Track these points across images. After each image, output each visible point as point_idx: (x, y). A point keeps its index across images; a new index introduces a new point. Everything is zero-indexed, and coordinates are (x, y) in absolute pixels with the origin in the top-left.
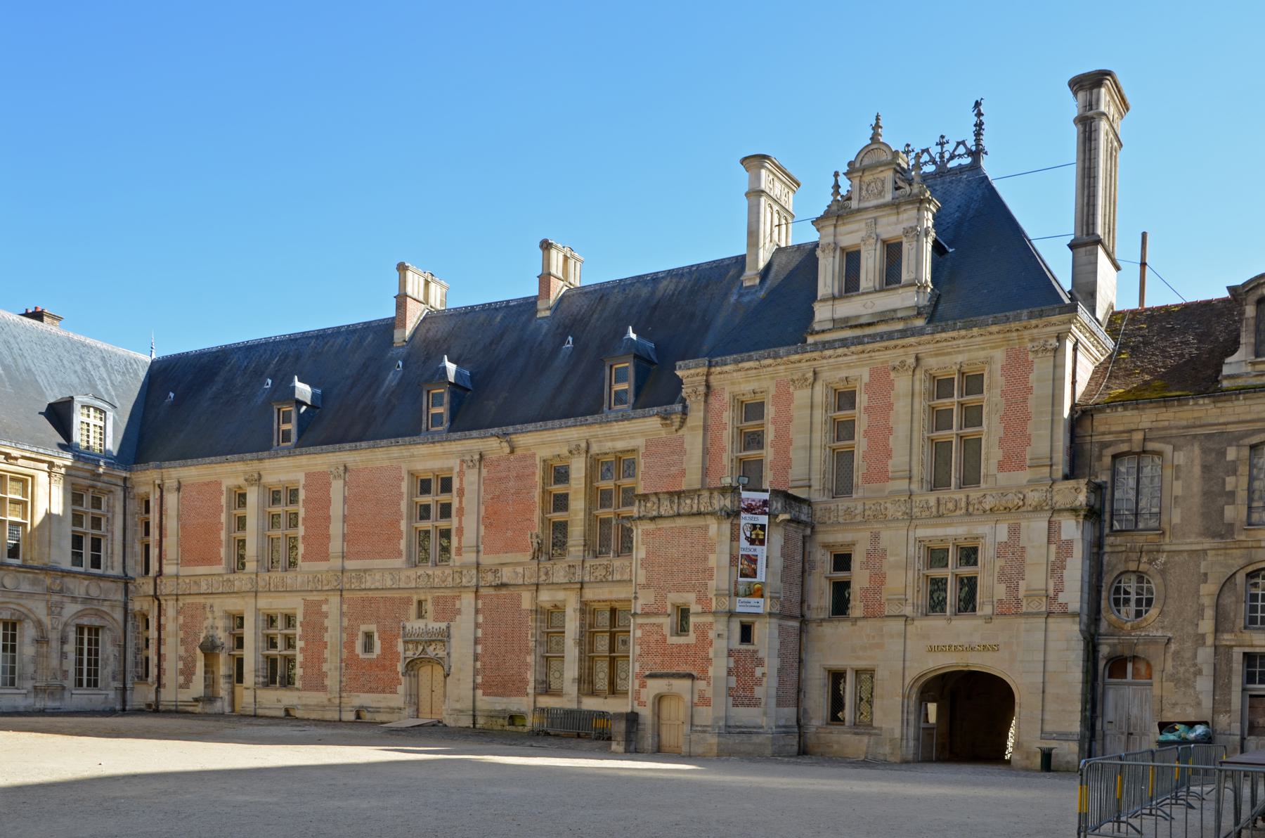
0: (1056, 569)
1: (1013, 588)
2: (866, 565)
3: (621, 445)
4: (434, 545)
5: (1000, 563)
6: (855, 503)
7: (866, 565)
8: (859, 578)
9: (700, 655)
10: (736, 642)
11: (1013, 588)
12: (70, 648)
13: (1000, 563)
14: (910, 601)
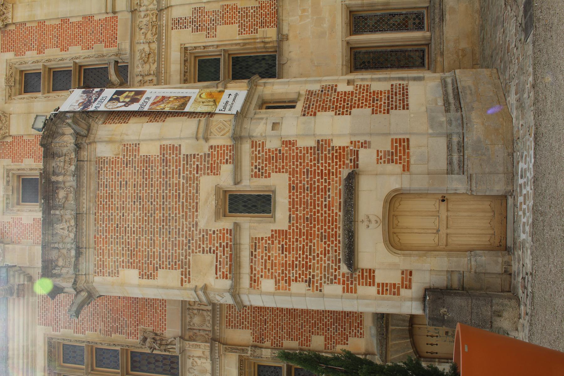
2: (210, 31)
7: (210, 31)
8: (228, 37)
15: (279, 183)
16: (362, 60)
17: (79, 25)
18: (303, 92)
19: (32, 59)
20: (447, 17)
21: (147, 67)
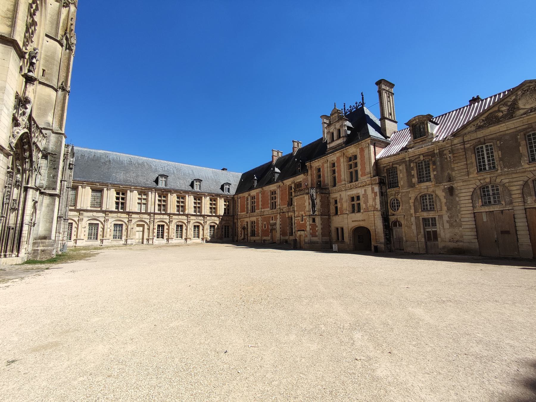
0: (374, 199)
1: (366, 205)
3: (299, 181)
4: (274, 206)
5: (363, 199)
9: (304, 225)
10: (311, 222)
11: (366, 205)
12: (224, 230)
13: (363, 199)
15: (303, 222)
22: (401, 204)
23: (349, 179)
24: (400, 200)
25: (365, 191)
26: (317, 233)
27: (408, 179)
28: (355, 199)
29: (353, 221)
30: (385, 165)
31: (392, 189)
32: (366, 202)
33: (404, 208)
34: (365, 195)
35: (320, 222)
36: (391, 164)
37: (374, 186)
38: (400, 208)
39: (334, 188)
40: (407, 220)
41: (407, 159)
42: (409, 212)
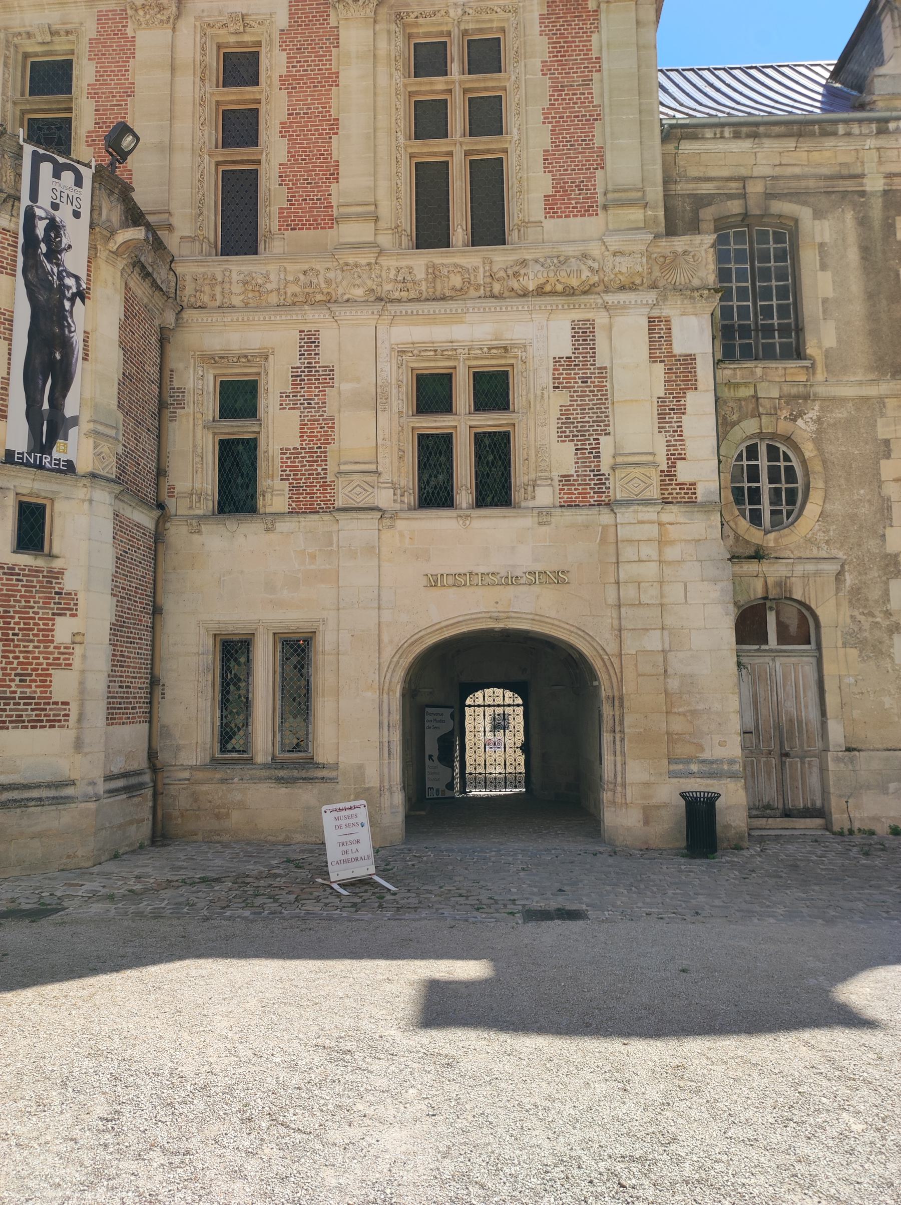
0: (669, 411)
1: (589, 453)
2: (291, 400)
5: (561, 399)
6: (276, 263)
7: (291, 400)
8: (278, 430)
11: (589, 453)
13: (561, 399)
14: (385, 477)
16: (234, 651)
17: (325, 155)
18: (57, 564)
19: (274, 64)
20: (283, 791)
21: (237, 288)
22: (817, 483)
23: (407, 221)
24: (809, 450)
25: (583, 335)
26: (63, 685)
27: (872, 316)
28: (463, 393)
29: (434, 582)
30: (706, 188)
31: (758, 368)
32: (586, 425)
33: (836, 507)
34: (582, 370)
35: (106, 559)
36: (755, 189)
37: (671, 310)
38: (812, 509)
39: (238, 267)
40: (856, 596)
41: (875, 184)
42: (872, 544)
